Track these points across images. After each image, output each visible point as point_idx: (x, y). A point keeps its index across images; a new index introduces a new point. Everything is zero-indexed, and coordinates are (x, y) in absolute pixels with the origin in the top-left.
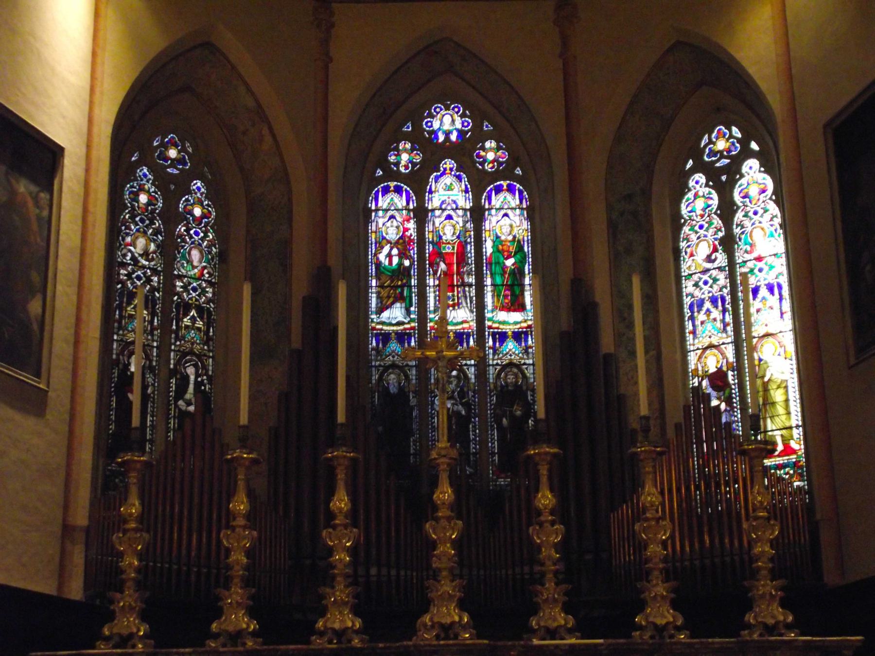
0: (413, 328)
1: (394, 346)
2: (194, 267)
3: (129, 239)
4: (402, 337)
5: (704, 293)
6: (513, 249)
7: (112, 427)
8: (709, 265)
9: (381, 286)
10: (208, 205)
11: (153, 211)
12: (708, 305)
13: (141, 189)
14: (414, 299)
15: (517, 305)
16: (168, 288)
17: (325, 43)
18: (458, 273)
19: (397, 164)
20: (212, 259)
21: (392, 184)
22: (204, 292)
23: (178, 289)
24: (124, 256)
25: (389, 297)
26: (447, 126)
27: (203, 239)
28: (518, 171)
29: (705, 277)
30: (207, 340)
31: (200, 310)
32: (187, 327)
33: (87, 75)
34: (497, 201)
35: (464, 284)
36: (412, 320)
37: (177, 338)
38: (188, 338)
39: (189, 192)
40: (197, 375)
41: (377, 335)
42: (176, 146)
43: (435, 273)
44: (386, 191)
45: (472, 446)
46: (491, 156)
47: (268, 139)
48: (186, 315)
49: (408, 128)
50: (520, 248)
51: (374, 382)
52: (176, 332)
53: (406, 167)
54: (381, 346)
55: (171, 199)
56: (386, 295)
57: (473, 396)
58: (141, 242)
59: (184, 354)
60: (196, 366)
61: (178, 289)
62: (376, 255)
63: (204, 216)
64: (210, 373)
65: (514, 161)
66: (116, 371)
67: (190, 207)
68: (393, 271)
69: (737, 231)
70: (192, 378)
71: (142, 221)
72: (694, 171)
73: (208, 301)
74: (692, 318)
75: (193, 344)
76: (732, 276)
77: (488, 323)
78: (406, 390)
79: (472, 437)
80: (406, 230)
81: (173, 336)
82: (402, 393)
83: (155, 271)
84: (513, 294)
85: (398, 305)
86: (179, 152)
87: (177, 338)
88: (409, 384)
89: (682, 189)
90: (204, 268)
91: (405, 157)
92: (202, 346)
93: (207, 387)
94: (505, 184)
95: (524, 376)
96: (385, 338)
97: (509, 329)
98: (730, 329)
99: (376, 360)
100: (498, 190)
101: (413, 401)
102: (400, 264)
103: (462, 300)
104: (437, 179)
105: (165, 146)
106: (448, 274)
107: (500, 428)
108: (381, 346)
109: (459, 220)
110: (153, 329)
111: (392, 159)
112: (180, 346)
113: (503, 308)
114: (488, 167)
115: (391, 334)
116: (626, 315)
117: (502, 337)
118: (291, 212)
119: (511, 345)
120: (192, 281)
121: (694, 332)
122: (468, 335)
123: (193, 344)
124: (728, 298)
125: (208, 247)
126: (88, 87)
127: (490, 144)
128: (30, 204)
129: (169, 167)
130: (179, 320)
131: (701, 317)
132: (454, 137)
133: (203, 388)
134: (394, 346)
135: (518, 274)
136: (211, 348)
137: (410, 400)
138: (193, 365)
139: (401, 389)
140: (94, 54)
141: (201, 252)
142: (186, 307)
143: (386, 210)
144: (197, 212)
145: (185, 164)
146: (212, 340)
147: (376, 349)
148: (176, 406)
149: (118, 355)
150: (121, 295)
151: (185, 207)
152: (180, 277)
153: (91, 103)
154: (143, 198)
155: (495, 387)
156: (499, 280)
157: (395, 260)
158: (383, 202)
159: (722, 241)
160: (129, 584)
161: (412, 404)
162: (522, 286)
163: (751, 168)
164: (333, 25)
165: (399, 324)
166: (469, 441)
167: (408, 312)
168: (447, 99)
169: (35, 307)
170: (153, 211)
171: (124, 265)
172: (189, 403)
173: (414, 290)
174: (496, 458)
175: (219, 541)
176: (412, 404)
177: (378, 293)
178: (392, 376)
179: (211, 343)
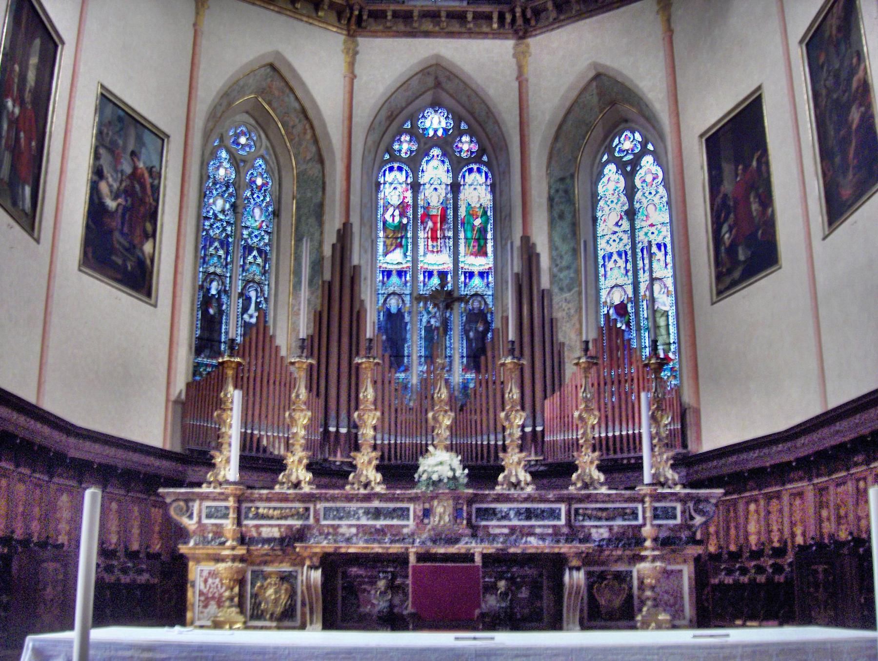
1: (394, 279)
2: (256, 221)
3: (211, 201)
4: (400, 273)
5: (614, 248)
6: (480, 212)
8: (616, 229)
9: (387, 237)
12: (615, 256)
14: (410, 247)
15: (482, 252)
17: (352, 64)
18: (441, 229)
19: (400, 151)
21: (396, 165)
22: (262, 238)
23: (245, 236)
24: (208, 212)
25: (392, 245)
26: (435, 126)
27: (262, 201)
28: (485, 158)
29: (614, 237)
31: (260, 251)
34: (469, 178)
35: (444, 237)
39: (253, 167)
40: (257, 298)
42: (245, 135)
43: (425, 228)
44: (391, 169)
46: (466, 147)
47: (309, 133)
48: (250, 254)
49: (408, 125)
50: (485, 213)
53: (406, 153)
58: (220, 202)
59: (249, 282)
60: (256, 290)
61: (245, 236)
62: (383, 214)
63: (263, 185)
65: (482, 151)
67: (253, 179)
68: (395, 227)
69: (637, 206)
70: (254, 299)
72: (607, 162)
73: (266, 245)
74: (604, 265)
76: (633, 237)
77: (461, 265)
80: (404, 198)
82: (400, 314)
83: (228, 223)
84: (479, 245)
86: (247, 139)
87: (243, 270)
89: (600, 174)
90: (263, 221)
91: (405, 146)
94: (475, 167)
95: (486, 303)
97: (476, 270)
98: (630, 273)
100: (471, 171)
102: (400, 222)
103: (443, 248)
104: (428, 161)
105: (237, 136)
106: (434, 230)
109: (442, 191)
111: (396, 147)
114: (464, 155)
116: (558, 262)
117: (471, 275)
118: (324, 183)
119: (477, 281)
121: (605, 276)
124: (629, 253)
125: (267, 207)
127: (466, 138)
128: (146, 175)
130: (245, 259)
131: (610, 265)
132: (440, 133)
134: (394, 279)
135: (483, 231)
139: (399, 310)
141: (261, 210)
143: (391, 184)
144: (259, 182)
145: (250, 148)
152: (247, 228)
156: (469, 235)
157: (397, 219)
158: (389, 177)
159: (627, 213)
162: (486, 239)
163: (648, 161)
164: (356, 53)
165: (398, 263)
167: (405, 255)
169: (148, 247)
172: (251, 316)
173: (410, 240)
177: (385, 242)
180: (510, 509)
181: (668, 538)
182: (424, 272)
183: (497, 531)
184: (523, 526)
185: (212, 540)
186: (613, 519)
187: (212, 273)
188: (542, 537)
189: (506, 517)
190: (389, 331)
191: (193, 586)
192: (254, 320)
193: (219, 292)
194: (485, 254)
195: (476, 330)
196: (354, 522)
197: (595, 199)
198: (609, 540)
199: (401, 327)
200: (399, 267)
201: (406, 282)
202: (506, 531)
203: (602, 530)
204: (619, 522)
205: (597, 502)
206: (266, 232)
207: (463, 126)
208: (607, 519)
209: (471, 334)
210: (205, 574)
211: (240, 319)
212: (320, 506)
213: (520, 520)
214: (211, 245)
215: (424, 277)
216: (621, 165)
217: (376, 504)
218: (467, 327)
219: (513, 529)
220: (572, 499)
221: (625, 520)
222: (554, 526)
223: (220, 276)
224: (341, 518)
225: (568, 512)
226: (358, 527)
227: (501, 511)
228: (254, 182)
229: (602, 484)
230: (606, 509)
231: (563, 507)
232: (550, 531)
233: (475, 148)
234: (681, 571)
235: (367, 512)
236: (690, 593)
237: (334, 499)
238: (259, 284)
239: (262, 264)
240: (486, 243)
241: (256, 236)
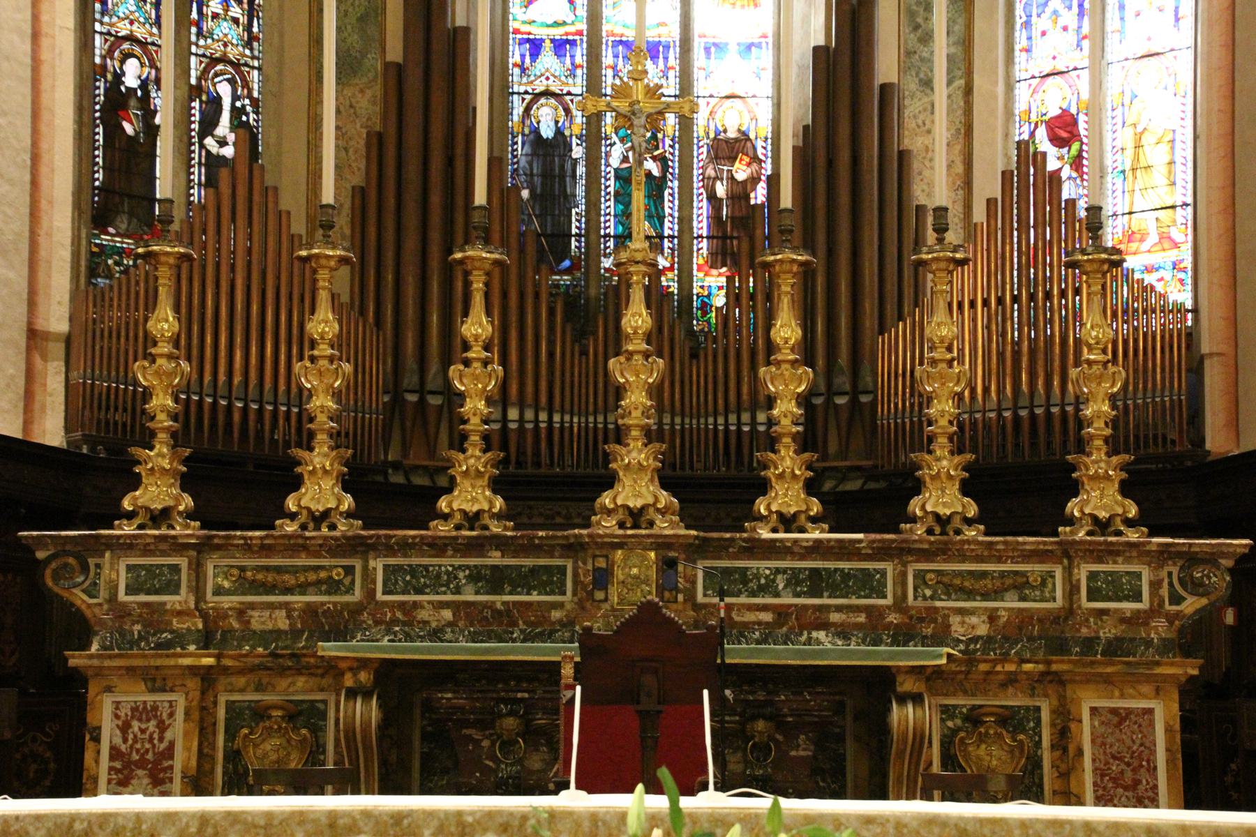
0: (580, 33)
1: (548, 60)
4: (560, 46)
7: (100, 175)
30: (250, 41)
32: (215, 16)
38: (218, 33)
40: (235, 97)
41: (522, 42)
45: (667, 224)
51: (516, 118)
54: (528, 60)
59: (214, 61)
60: (232, 82)
64: (256, 94)
66: (101, 84)
74: (1027, 25)
75: (225, 45)
77: (698, 27)
78: (567, 133)
79: (667, 211)
81: (194, 30)
82: (560, 141)
87: (200, 34)
88: (571, 123)
92: (240, 48)
93: (252, 116)
96: (535, 46)
99: (520, 84)
101: (578, 152)
107: (712, 197)
108: (528, 60)
115: (543, 40)
116: (920, 20)
122: (667, 47)
123: (225, 45)
131: (1039, 24)
133: (244, 118)
134: (548, 60)
137: (571, 150)
138: (228, 80)
139: (559, 132)
146: (258, 39)
148: (202, 146)
149: (103, 57)
160: (162, 436)
161: (574, 156)
165: (556, 24)
172: (222, 143)
174: (704, 244)
175: (301, 389)
176: (574, 156)
179: (255, 44)
180: (778, 571)
181: (1118, 639)
183: (750, 617)
184: (805, 607)
185: (141, 638)
186: (997, 594)
188: (843, 632)
189: (768, 588)
190: (537, 181)
191: (97, 739)
193: (144, 84)
195: (732, 178)
196: (449, 597)
198: (988, 640)
199: (562, 167)
200: (558, 33)
201: (575, 66)
202: (767, 617)
203: (974, 620)
204: (1011, 603)
205: (963, 558)
208: (986, 596)
209: (721, 190)
210: (125, 711)
211: (196, 148)
212: (378, 565)
213: (798, 595)
215: (616, 56)
217: (495, 558)
218: (710, 172)
219: (782, 614)
220: (910, 551)
221: (1023, 599)
222: (868, 609)
223: (143, 44)
224: (419, 591)
225: (901, 580)
226: (455, 606)
227: (757, 576)
229: (969, 522)
230: (984, 574)
231: (889, 567)
232: (862, 618)
234: (1150, 711)
235: (476, 576)
236: (1170, 761)
237: (405, 547)
239: (243, 20)
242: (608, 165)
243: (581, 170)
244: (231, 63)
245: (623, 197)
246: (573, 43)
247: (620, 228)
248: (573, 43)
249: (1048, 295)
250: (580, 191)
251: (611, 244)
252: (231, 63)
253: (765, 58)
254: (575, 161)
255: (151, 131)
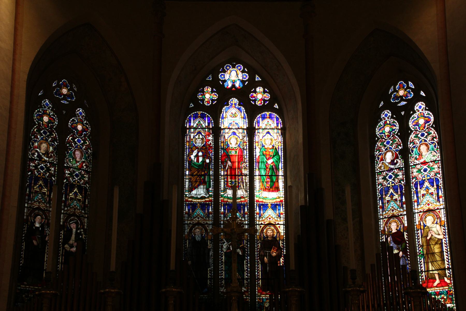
1: (199, 211)
2: (77, 162)
4: (204, 206)
6: (272, 152)
8: (392, 167)
9: (191, 175)
10: (86, 124)
11: (52, 127)
13: (45, 113)
14: (212, 183)
15: (274, 188)
16: (61, 174)
20: (89, 157)
21: (199, 113)
22: (83, 177)
24: (33, 154)
25: (196, 182)
27: (83, 145)
28: (276, 106)
30: (84, 207)
31: (80, 188)
32: (71, 198)
33: (12, 43)
34: (263, 124)
35: (242, 175)
36: (210, 196)
37: (65, 206)
39: (75, 115)
40: (77, 229)
41: (188, 205)
42: (67, 87)
43: (225, 167)
44: (196, 117)
45: (246, 274)
46: (260, 96)
49: (210, 78)
50: (277, 153)
51: (186, 233)
52: (65, 202)
54: (191, 211)
55: (63, 120)
56: (194, 180)
57: (247, 243)
58: (44, 146)
59: (70, 215)
62: (189, 155)
63: (83, 130)
64: (86, 227)
68: (199, 165)
70: (74, 230)
71: (45, 133)
72: (384, 108)
73: (85, 183)
74: (382, 198)
75: (75, 209)
77: (256, 199)
78: (206, 239)
79: (245, 268)
81: (63, 204)
82: (204, 240)
83: (52, 164)
84: (272, 181)
85: (202, 186)
86: (69, 90)
87: (65, 206)
88: (208, 235)
90: (84, 162)
91: (207, 96)
95: (278, 232)
96: (194, 206)
99: (188, 220)
101: (210, 246)
102: (204, 161)
108: (191, 211)
109: (241, 134)
110: (50, 200)
112: (67, 210)
113: (265, 190)
114: (258, 103)
117: (264, 206)
120: (75, 170)
121: (383, 207)
122: (244, 206)
123: (75, 209)
125: (86, 149)
126: (12, 49)
129: (62, 99)
133: (81, 237)
134: (199, 211)
135: (275, 169)
136: (87, 212)
137: (208, 245)
139: (203, 238)
140: (16, 29)
141: (81, 152)
142: (71, 186)
143: (195, 129)
144: (80, 127)
145: (72, 98)
146: (87, 206)
147: (188, 213)
148: (64, 248)
150: (31, 179)
151: (72, 124)
152: (68, 168)
153: (14, 60)
154: (46, 119)
155: (260, 238)
156: (263, 173)
157: (201, 159)
158: (194, 124)
159: (401, 152)
163: (420, 106)
165: (202, 198)
166: (243, 271)
168: (233, 62)
170: (52, 127)
171: (33, 160)
172: (72, 246)
174: (260, 282)
177: (190, 179)
178: (198, 230)
182: (224, 205)
187: (37, 208)
192: (74, 249)
193: (42, 226)
194: (277, 189)
195: (270, 255)
197: (373, 139)
206: (86, 171)
207: (258, 78)
214: (35, 184)
215: (224, 209)
216: (396, 111)
218: (262, 253)
223: (43, 211)
228: (76, 128)
233: (267, 96)
238: (79, 217)
240: (277, 180)
241: (77, 176)
242: (222, 251)
243: (211, 253)
244: (77, 216)
245: (228, 263)
246: (208, 205)
247: (227, 275)
248: (208, 205)
249: (398, 304)
250: (211, 261)
251: (223, 282)
252: (77, 216)
253: (282, 210)
254: (209, 250)
255: (44, 243)
